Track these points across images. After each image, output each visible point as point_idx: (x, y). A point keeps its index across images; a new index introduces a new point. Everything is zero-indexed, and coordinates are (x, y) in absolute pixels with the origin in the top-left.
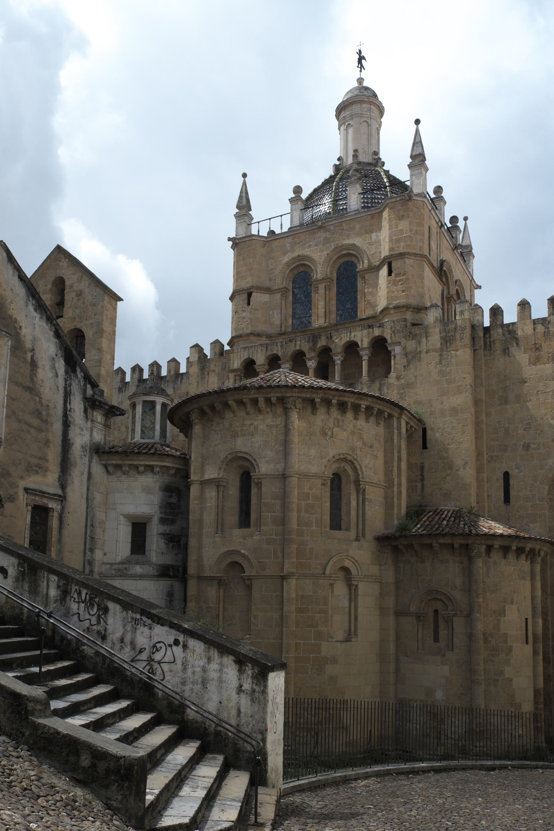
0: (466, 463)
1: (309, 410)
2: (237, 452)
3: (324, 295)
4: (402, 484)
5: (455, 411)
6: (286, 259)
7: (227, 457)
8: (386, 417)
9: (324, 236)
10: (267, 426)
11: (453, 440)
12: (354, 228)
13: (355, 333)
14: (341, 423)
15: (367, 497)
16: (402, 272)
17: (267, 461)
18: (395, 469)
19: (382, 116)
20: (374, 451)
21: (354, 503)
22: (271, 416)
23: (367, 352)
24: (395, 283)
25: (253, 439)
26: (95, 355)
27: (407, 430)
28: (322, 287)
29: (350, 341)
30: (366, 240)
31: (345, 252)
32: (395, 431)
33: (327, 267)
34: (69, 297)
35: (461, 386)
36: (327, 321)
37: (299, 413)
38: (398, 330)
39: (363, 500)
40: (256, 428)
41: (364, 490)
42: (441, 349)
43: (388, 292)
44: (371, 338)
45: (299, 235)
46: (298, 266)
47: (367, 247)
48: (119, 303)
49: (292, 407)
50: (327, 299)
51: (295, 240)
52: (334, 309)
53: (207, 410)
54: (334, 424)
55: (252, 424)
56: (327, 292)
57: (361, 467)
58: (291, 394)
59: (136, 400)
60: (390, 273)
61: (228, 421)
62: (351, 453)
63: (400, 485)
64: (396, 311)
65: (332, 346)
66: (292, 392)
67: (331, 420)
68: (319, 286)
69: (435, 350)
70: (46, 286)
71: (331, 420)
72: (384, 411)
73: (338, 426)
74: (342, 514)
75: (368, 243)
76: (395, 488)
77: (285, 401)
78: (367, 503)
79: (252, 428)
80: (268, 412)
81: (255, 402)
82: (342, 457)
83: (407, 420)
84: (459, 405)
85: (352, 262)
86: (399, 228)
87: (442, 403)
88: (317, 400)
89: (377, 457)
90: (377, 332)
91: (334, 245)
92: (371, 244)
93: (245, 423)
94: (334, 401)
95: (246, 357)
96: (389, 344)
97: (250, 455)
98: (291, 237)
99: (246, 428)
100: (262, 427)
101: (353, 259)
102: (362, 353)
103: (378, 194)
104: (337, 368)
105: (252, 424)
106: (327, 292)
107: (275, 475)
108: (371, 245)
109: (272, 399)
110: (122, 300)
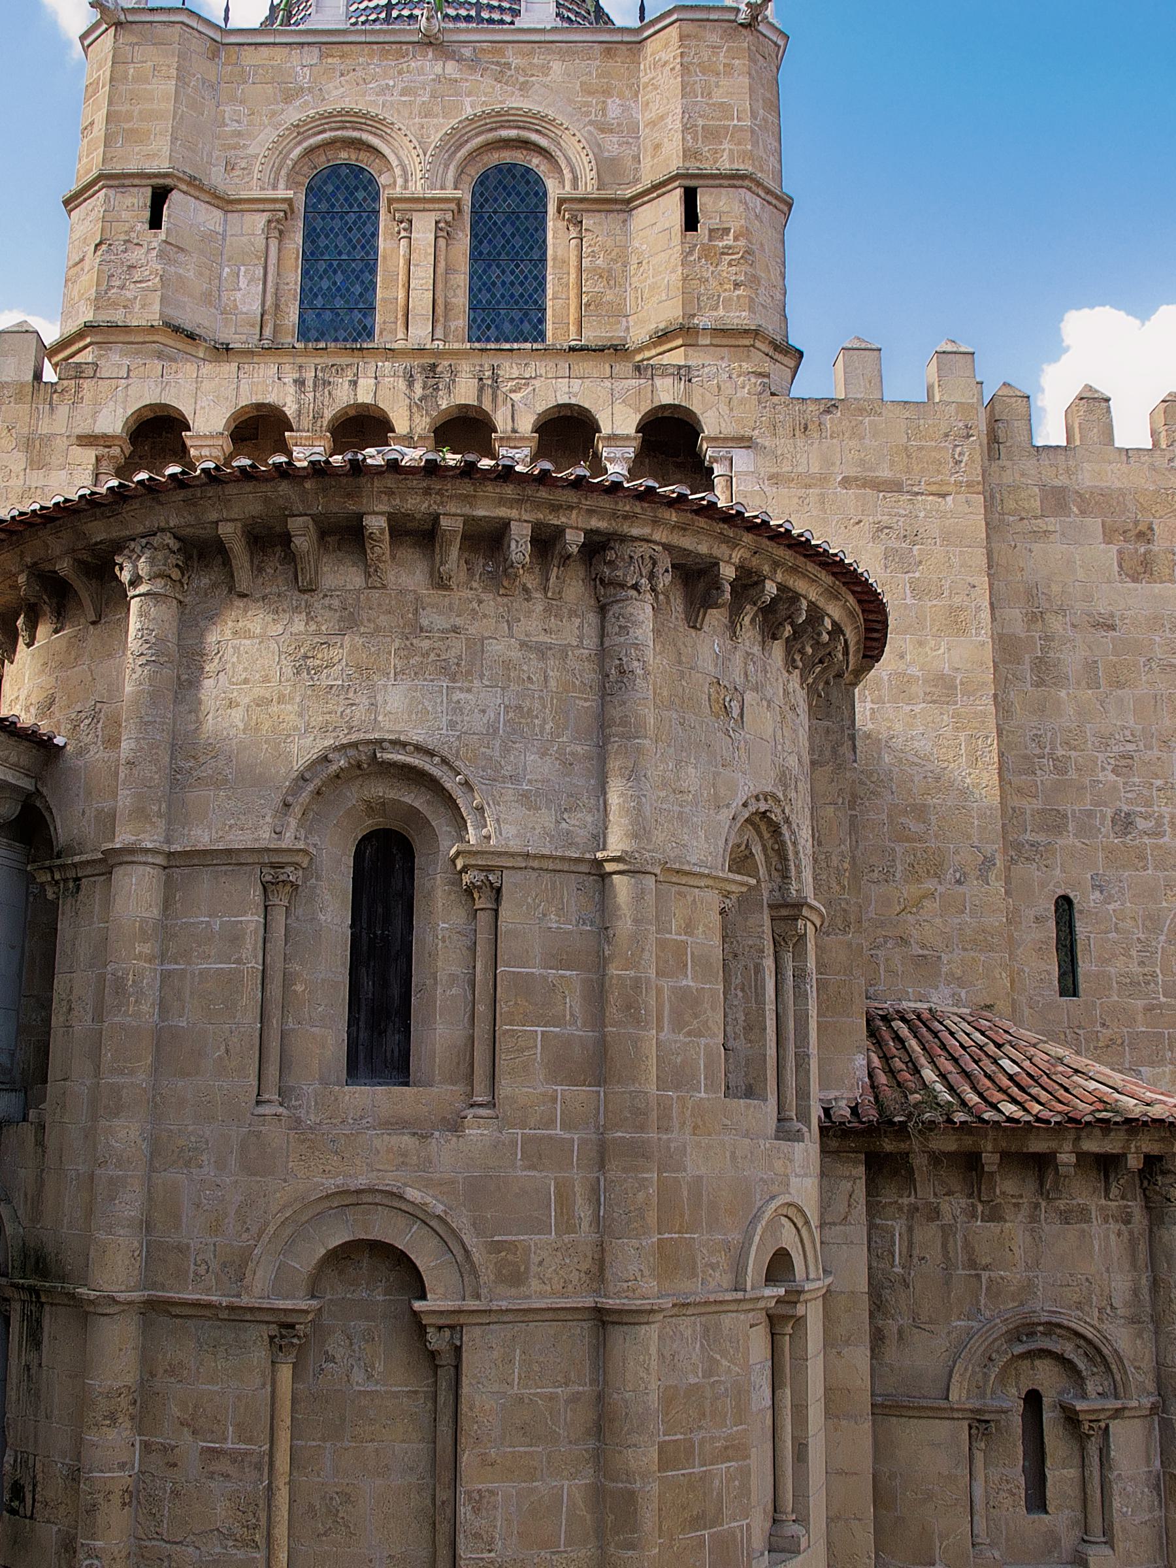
0: (988, 862)
2: (379, 742)
6: (293, 114)
7: (325, 759)
9: (438, 69)
10: (523, 644)
12: (545, 69)
16: (734, 226)
17: (525, 795)
22: (539, 608)
24: (708, 253)
25: (458, 696)
30: (588, 114)
31: (513, 133)
33: (447, 166)
36: (439, 333)
40: (477, 646)
43: (685, 279)
44: (646, 407)
45: (346, 48)
46: (332, 143)
47: (590, 132)
50: (442, 265)
51: (330, 60)
52: (461, 300)
54: (746, 674)
55: (455, 630)
56: (442, 242)
58: (645, 531)
60: (691, 222)
61: (336, 603)
62: (780, 795)
64: (716, 341)
66: (655, 522)
67: (738, 657)
68: (416, 217)
71: (738, 657)
73: (756, 689)
75: (591, 123)
79: (458, 646)
80: (526, 590)
85: (528, 170)
90: (667, 393)
93: (425, 622)
97: (445, 761)
98: (315, 50)
99: (426, 644)
100: (497, 648)
101: (535, 162)
103: (569, 10)
106: (442, 242)
107: (563, 859)
108: (602, 131)
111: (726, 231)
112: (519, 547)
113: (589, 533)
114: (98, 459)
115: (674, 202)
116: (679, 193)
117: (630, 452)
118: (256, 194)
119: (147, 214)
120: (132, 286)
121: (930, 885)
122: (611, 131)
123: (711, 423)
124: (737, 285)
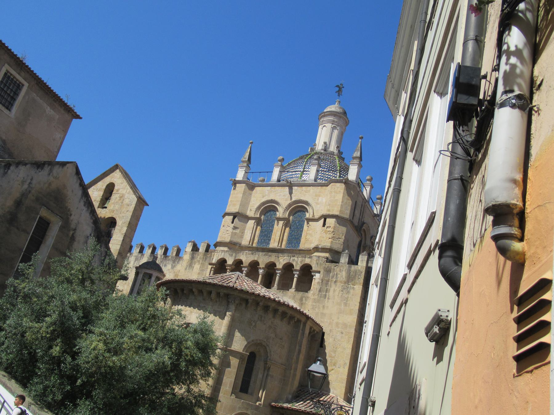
1: (244, 305)
3: (281, 228)
4: (298, 369)
5: (345, 325)
8: (296, 321)
11: (340, 345)
13: (294, 258)
14: (263, 318)
15: (270, 373)
18: (295, 357)
19: (347, 125)
20: (283, 342)
21: (260, 376)
23: (298, 273)
24: (326, 232)
26: (119, 237)
27: (310, 333)
28: (281, 223)
29: (289, 263)
32: (300, 331)
34: (115, 197)
35: (352, 310)
37: (236, 307)
38: (321, 264)
39: (267, 375)
41: (269, 368)
42: (345, 283)
48: (146, 207)
49: (232, 301)
53: (179, 291)
54: (258, 318)
55: (204, 307)
57: (271, 352)
59: (140, 271)
60: (324, 225)
63: (296, 369)
65: (277, 264)
68: (280, 222)
69: (341, 282)
70: (102, 186)
72: (295, 317)
74: (251, 382)
76: (292, 371)
77: (229, 297)
78: (269, 378)
81: (210, 293)
82: (259, 342)
83: (311, 325)
84: (349, 322)
86: (336, 198)
87: (338, 318)
88: (250, 301)
89: (284, 346)
90: (307, 261)
91: (295, 198)
92: (317, 204)
93: (200, 305)
94: (261, 304)
95: (221, 257)
96: (313, 271)
102: (294, 272)
104: (277, 278)
105: (204, 307)
109: (221, 294)
110: (148, 205)
111: (330, 227)
112: (213, 295)
113: (224, 293)
114: (212, 268)
115: (322, 221)
116: (323, 219)
117: (298, 273)
118: (253, 216)
119: (231, 221)
120: (226, 234)
121: (334, 367)
122: (319, 204)
123: (314, 268)
124: (330, 238)
